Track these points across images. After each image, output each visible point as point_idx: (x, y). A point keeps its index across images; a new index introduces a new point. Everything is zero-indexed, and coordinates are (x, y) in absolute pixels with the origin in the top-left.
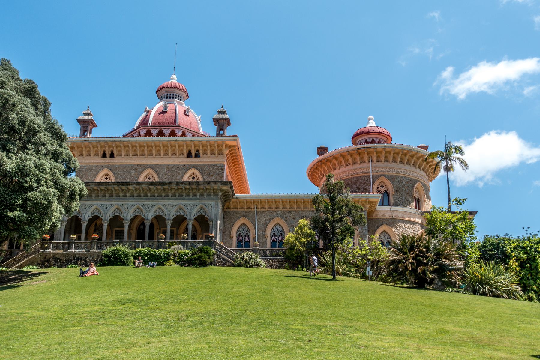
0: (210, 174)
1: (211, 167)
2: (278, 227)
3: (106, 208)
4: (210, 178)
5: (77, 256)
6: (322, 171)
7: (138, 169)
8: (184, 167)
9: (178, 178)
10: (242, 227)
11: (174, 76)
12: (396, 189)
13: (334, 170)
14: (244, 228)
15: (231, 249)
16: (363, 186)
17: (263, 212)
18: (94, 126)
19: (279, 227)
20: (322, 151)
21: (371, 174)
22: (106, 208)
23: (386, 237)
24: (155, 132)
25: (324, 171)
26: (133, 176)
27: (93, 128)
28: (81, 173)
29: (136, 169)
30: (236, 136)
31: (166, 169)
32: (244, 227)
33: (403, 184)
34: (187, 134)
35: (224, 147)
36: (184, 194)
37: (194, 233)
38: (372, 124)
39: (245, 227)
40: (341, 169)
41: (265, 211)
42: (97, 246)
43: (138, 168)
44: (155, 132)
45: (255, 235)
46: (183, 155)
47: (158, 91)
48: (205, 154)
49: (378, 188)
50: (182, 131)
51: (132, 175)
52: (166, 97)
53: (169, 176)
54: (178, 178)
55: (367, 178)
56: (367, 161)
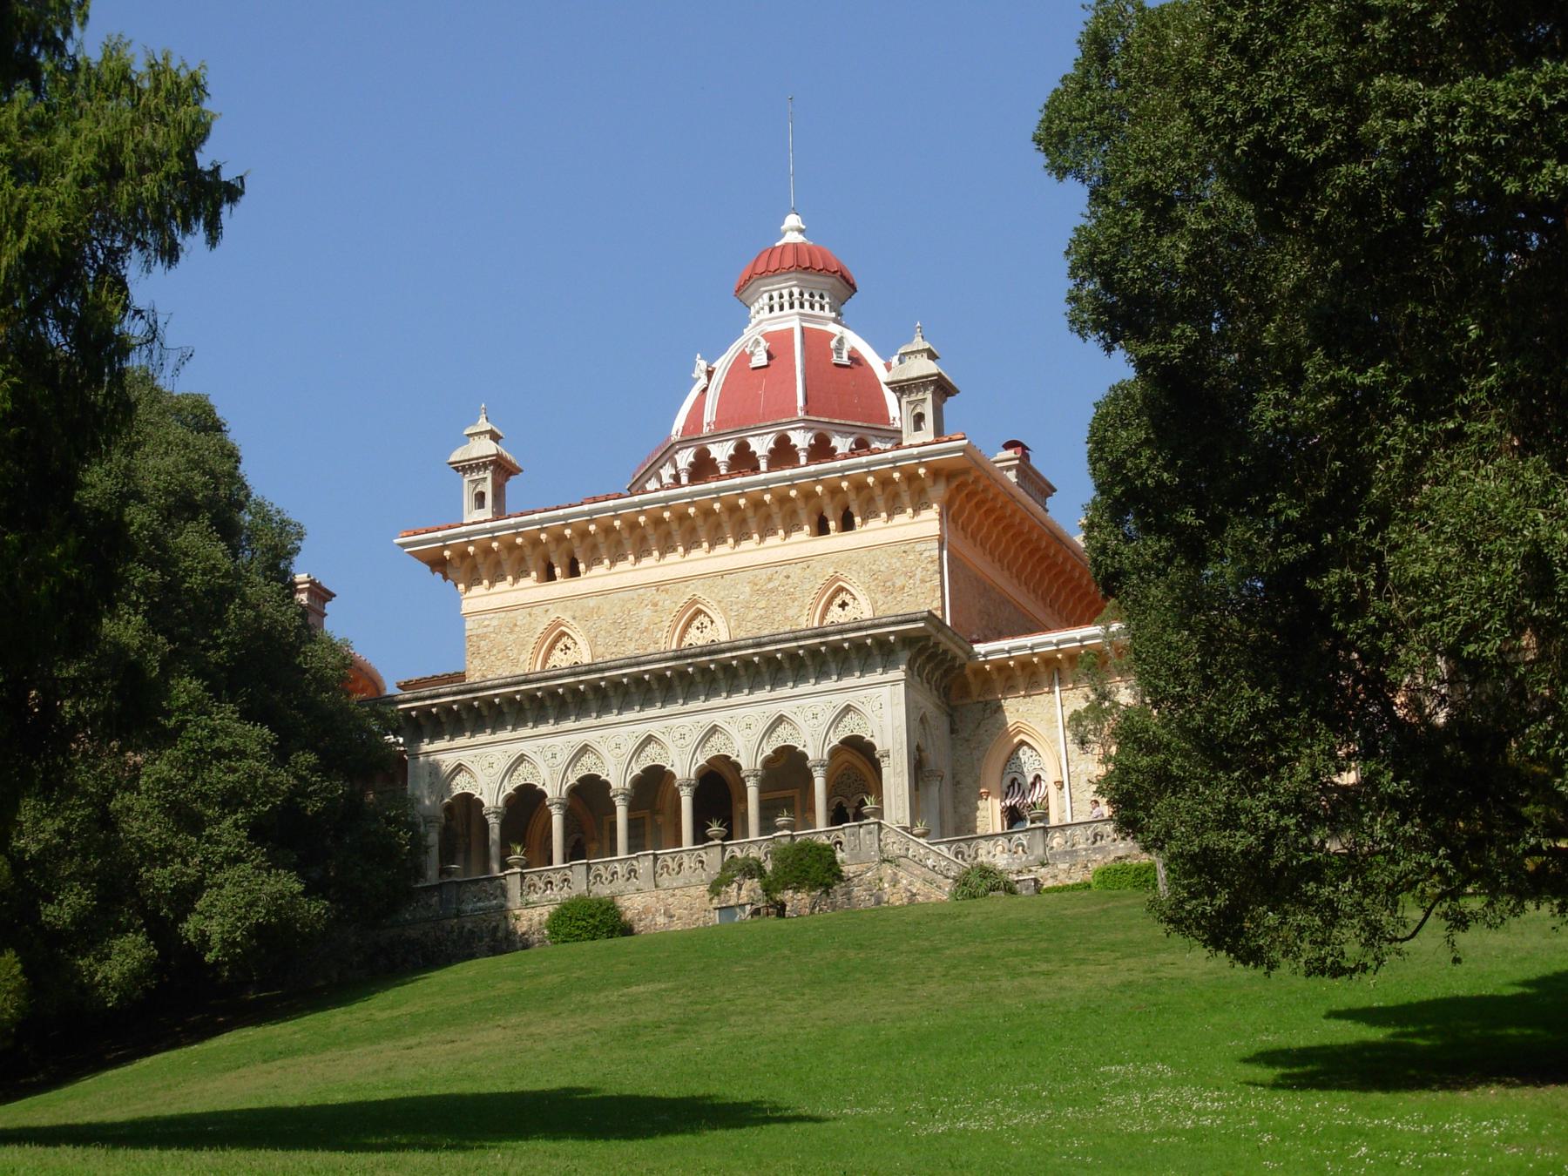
1: (894, 560)
5: (469, 926)
7: (660, 604)
9: (790, 613)
18: (512, 473)
24: (721, 452)
26: (646, 630)
27: (507, 480)
28: (483, 643)
29: (656, 605)
31: (748, 589)
35: (929, 482)
37: (838, 800)
43: (658, 598)
44: (721, 452)
47: (739, 289)
51: (642, 627)
52: (767, 308)
53: (762, 612)
54: (790, 613)
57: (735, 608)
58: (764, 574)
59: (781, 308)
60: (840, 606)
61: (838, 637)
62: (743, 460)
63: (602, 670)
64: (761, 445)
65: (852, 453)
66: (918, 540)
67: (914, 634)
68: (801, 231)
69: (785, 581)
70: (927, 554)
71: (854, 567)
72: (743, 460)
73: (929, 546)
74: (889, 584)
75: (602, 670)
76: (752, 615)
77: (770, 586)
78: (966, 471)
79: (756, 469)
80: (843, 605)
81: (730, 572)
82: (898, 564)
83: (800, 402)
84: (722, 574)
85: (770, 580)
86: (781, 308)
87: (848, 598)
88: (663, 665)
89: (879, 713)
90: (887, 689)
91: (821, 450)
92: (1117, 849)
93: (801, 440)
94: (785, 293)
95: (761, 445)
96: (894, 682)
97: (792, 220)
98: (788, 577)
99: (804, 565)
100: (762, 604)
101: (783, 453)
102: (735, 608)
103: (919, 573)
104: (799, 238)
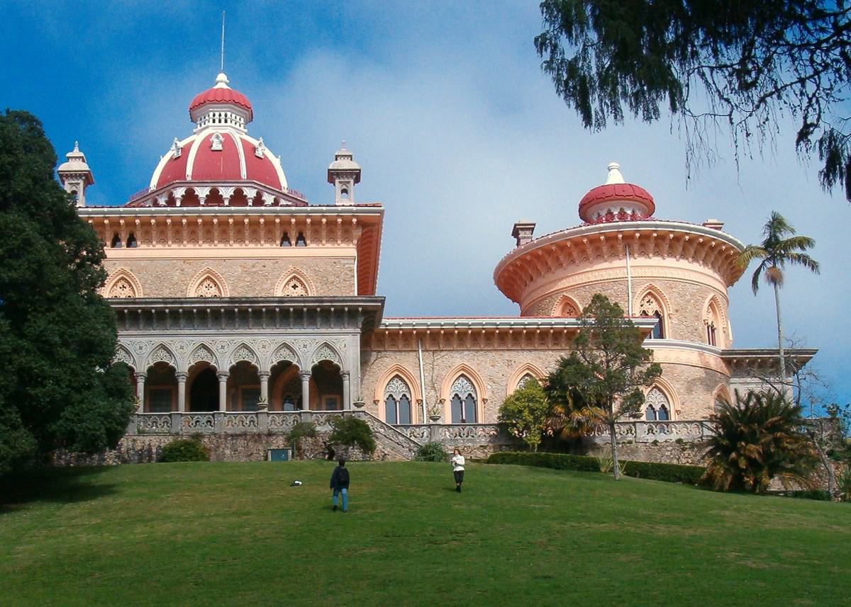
0: (327, 280)
2: (463, 382)
3: (141, 348)
4: (328, 287)
7: (186, 270)
8: (277, 265)
10: (394, 382)
11: (222, 77)
12: (676, 308)
14: (398, 384)
19: (465, 382)
21: (630, 279)
22: (141, 348)
23: (658, 398)
26: (177, 283)
31: (240, 270)
32: (397, 382)
33: (688, 297)
34: (283, 202)
38: (615, 178)
39: (400, 382)
43: (184, 267)
45: (420, 398)
49: (642, 306)
50: (256, 190)
51: (174, 282)
52: (211, 120)
54: (264, 286)
55: (621, 286)
57: (232, 279)
58: (250, 263)
59: (220, 121)
60: (293, 287)
61: (329, 304)
62: (214, 198)
63: (182, 303)
64: (226, 192)
65: (273, 205)
66: (344, 258)
67: (370, 309)
68: (226, 83)
69: (264, 269)
70: (347, 266)
71: (305, 267)
72: (214, 198)
73: (349, 262)
74: (325, 279)
75: (182, 303)
76: (241, 285)
77: (254, 270)
78: (373, 225)
79: (198, 204)
80: (295, 287)
81: (230, 259)
82: (331, 269)
83: (244, 173)
84: (225, 259)
85: (253, 266)
86: (220, 121)
87: (298, 284)
88: (317, 304)
89: (344, 349)
90: (349, 338)
91: (258, 201)
92: (481, 441)
93: (250, 193)
94: (223, 114)
95: (226, 192)
96: (354, 334)
97: (222, 77)
98: (264, 266)
99: (274, 261)
100: (248, 279)
101: (238, 198)
102: (232, 279)
103: (342, 276)
104: (225, 87)
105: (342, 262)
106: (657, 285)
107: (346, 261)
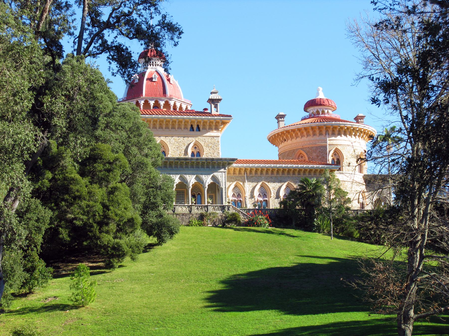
6: (285, 137)
13: (296, 138)
15: (241, 209)
16: (321, 155)
17: (251, 177)
20: (280, 117)
25: (286, 137)
30: (230, 116)
35: (220, 124)
36: (200, 166)
38: (321, 96)
40: (303, 138)
41: (253, 177)
42: (421, 286)
46: (187, 129)
48: (204, 128)
56: (324, 135)
77: (180, 141)
105: (215, 138)
106: (339, 148)
107: (216, 138)
